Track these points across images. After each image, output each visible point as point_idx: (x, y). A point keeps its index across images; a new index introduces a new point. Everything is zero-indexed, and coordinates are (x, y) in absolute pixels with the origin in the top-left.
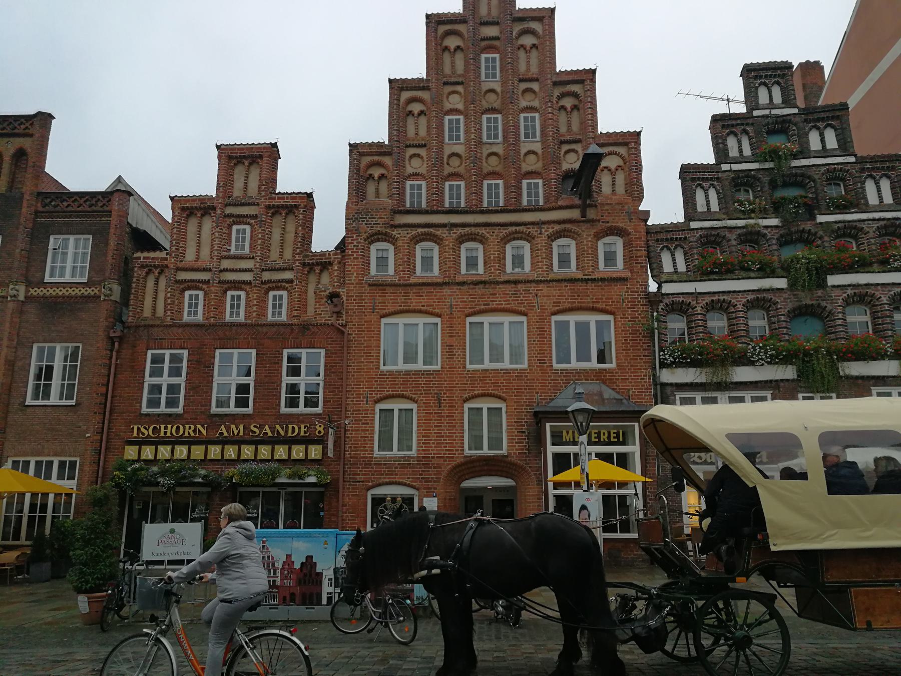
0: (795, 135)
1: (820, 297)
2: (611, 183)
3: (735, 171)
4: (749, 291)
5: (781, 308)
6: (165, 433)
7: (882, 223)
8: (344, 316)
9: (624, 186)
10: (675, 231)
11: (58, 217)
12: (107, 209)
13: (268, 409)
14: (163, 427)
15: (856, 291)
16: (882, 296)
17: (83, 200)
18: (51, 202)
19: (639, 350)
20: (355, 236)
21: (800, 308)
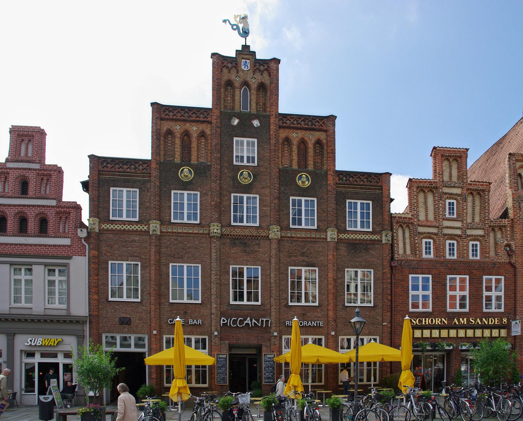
6: (425, 323)
8: (514, 259)
12: (379, 184)
13: (477, 309)
14: (424, 319)
20: (518, 210)
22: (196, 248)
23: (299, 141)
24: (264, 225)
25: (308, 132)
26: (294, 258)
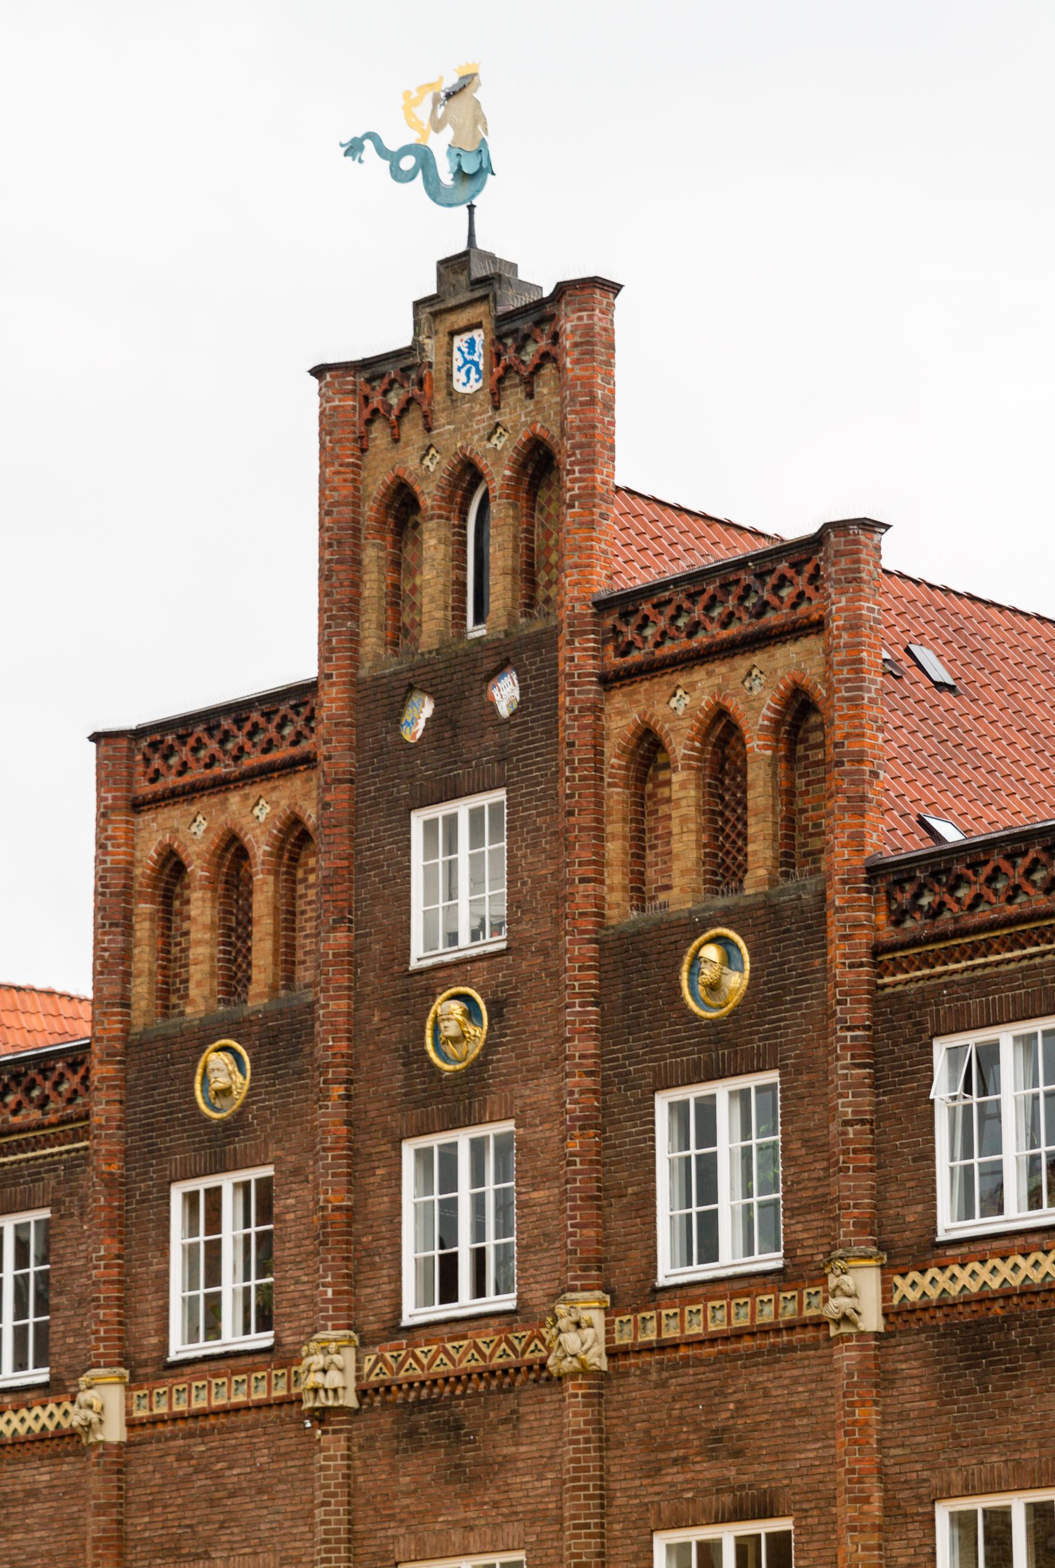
11: (949, 956)
17: (1023, 863)
18: (918, 896)
22: (260, 1491)
23: (705, 734)
24: (537, 1295)
25: (742, 664)
26: (673, 1475)
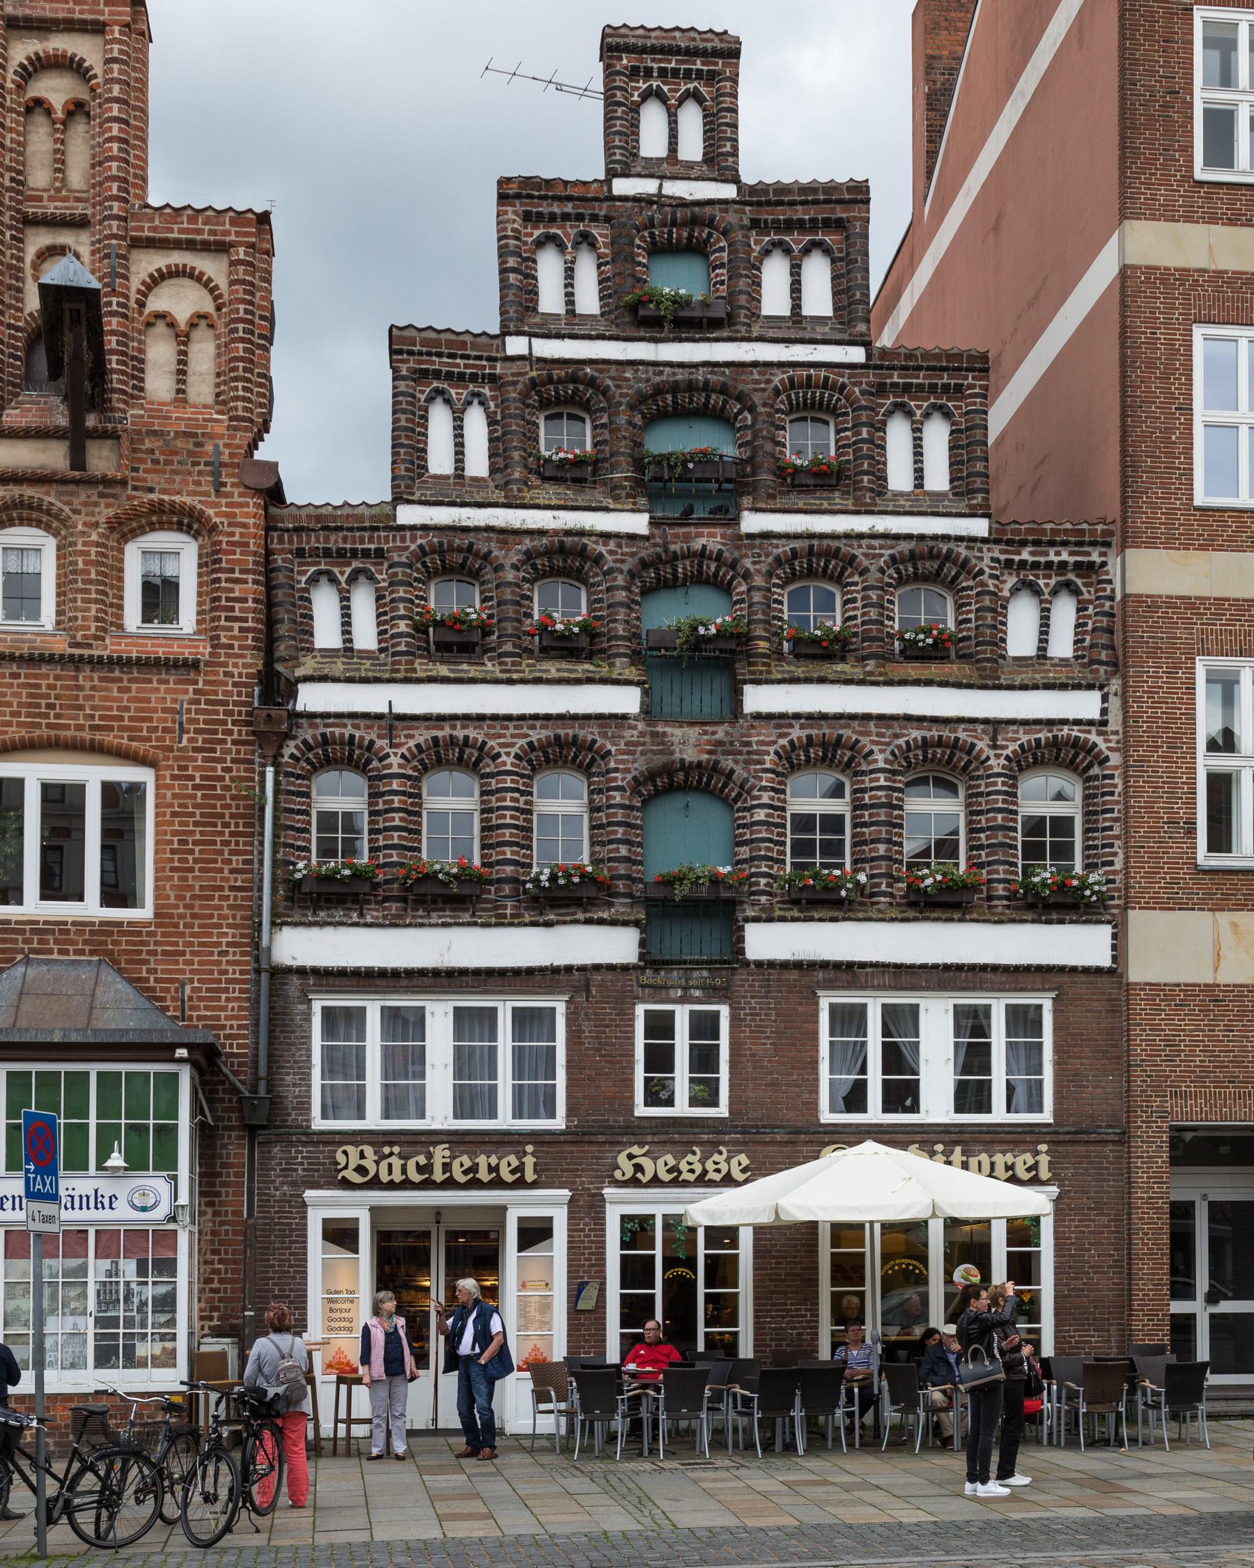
0: (722, 266)
1: (720, 743)
2: (174, 367)
3: (541, 360)
4: (535, 717)
5: (616, 770)
7: (905, 546)
9: (212, 380)
10: (351, 529)
15: (814, 732)
16: (875, 748)
19: (221, 871)
21: (668, 770)
